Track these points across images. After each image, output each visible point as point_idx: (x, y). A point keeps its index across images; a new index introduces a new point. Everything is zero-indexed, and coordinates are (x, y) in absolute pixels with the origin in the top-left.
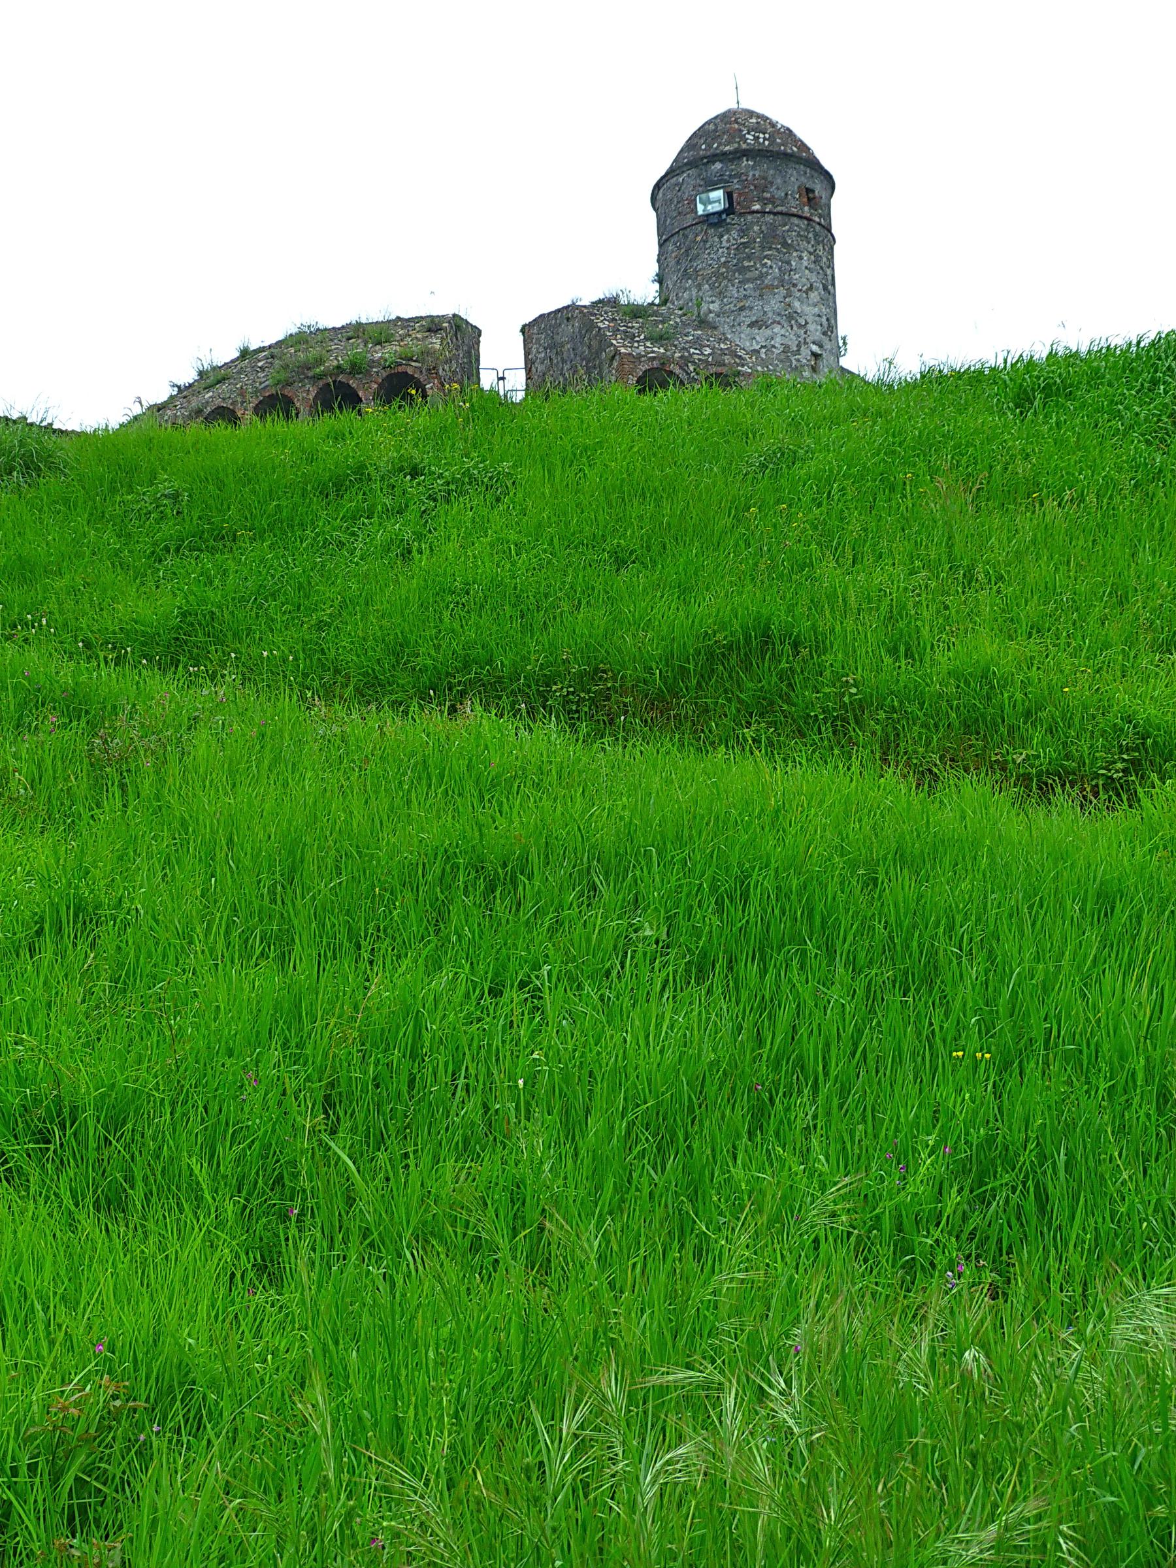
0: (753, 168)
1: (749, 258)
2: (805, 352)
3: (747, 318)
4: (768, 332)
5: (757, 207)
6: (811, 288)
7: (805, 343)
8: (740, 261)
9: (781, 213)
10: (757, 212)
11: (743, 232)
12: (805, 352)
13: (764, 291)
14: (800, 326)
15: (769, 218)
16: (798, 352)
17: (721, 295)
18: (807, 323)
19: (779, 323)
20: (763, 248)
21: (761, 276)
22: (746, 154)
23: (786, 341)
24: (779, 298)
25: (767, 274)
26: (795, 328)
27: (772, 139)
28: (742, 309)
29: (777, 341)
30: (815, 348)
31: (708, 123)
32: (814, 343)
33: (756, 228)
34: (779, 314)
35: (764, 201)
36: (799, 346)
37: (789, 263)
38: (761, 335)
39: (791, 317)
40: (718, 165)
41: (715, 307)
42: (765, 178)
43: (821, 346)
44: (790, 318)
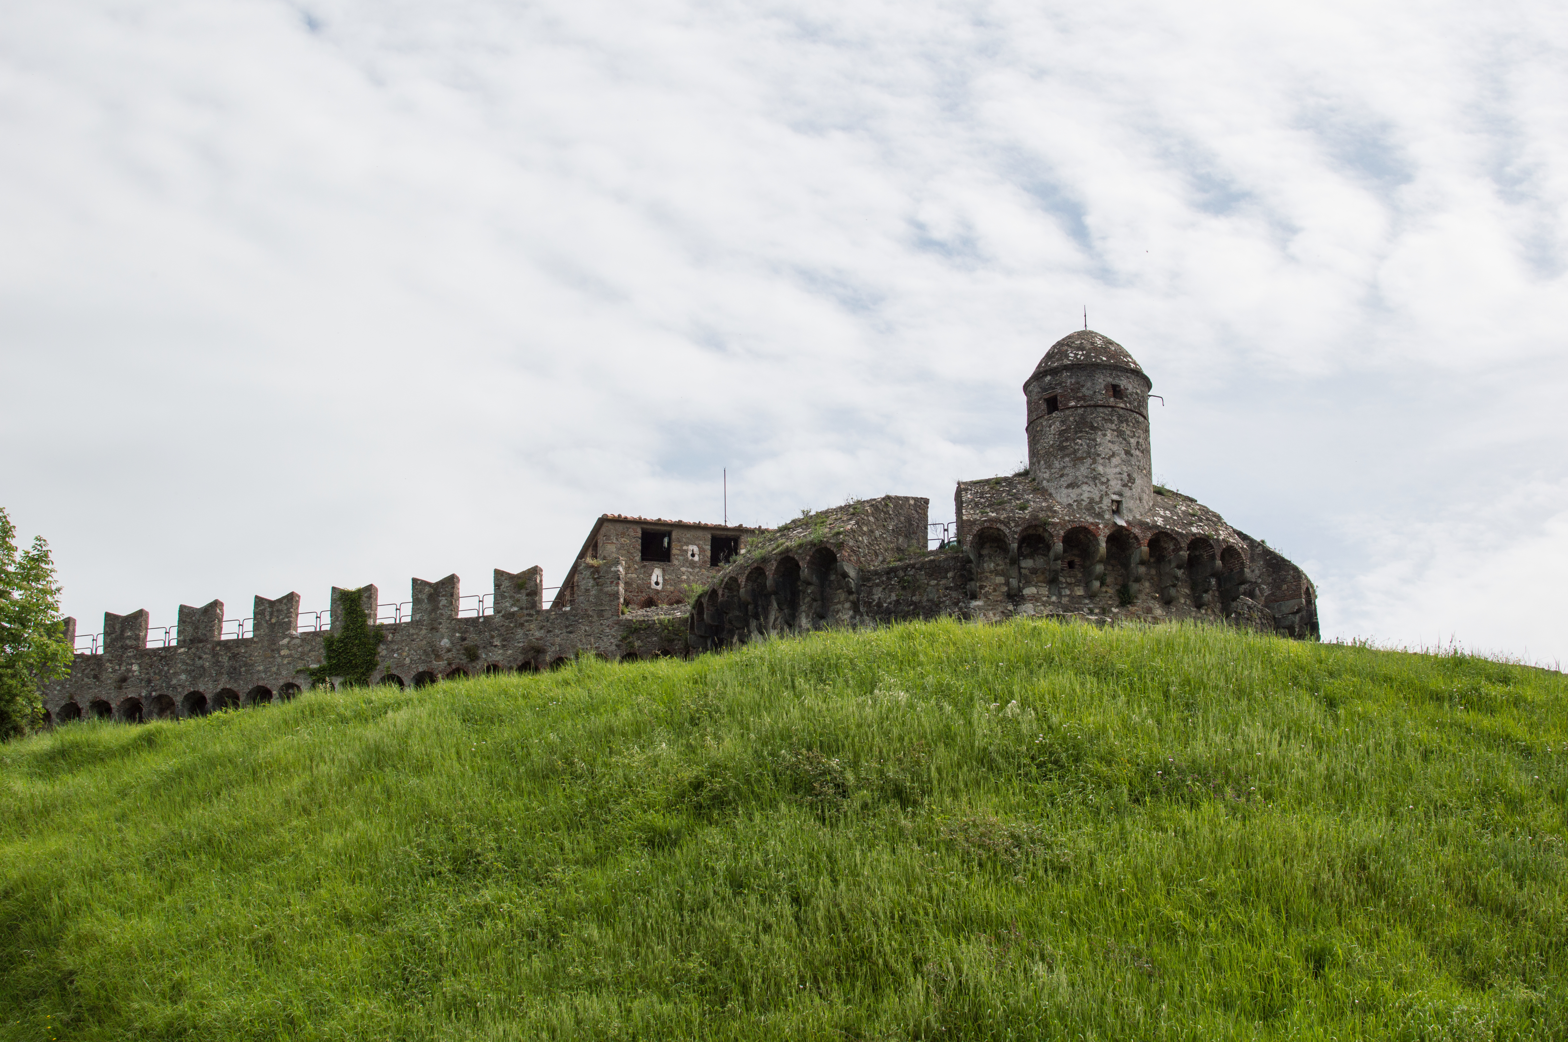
0: (1070, 377)
1: (1067, 440)
2: (1106, 502)
3: (1064, 481)
4: (1077, 491)
5: (1073, 404)
6: (1113, 455)
7: (1107, 494)
8: (1061, 442)
9: (1089, 406)
10: (1072, 407)
11: (1063, 422)
12: (1106, 502)
13: (1077, 460)
14: (1102, 483)
15: (1081, 411)
16: (1101, 501)
17: (1049, 466)
18: (1108, 480)
20: (1076, 433)
22: (1066, 368)
23: (1091, 495)
24: (1087, 465)
27: (1087, 356)
28: (1062, 476)
30: (1115, 497)
31: (1054, 347)
35: (1078, 399)
36: (1101, 498)
37: (1094, 440)
38: (1074, 493)
39: (1095, 478)
40: (1049, 378)
41: (1047, 476)
42: (1078, 383)
43: (1121, 495)
44: (1095, 478)
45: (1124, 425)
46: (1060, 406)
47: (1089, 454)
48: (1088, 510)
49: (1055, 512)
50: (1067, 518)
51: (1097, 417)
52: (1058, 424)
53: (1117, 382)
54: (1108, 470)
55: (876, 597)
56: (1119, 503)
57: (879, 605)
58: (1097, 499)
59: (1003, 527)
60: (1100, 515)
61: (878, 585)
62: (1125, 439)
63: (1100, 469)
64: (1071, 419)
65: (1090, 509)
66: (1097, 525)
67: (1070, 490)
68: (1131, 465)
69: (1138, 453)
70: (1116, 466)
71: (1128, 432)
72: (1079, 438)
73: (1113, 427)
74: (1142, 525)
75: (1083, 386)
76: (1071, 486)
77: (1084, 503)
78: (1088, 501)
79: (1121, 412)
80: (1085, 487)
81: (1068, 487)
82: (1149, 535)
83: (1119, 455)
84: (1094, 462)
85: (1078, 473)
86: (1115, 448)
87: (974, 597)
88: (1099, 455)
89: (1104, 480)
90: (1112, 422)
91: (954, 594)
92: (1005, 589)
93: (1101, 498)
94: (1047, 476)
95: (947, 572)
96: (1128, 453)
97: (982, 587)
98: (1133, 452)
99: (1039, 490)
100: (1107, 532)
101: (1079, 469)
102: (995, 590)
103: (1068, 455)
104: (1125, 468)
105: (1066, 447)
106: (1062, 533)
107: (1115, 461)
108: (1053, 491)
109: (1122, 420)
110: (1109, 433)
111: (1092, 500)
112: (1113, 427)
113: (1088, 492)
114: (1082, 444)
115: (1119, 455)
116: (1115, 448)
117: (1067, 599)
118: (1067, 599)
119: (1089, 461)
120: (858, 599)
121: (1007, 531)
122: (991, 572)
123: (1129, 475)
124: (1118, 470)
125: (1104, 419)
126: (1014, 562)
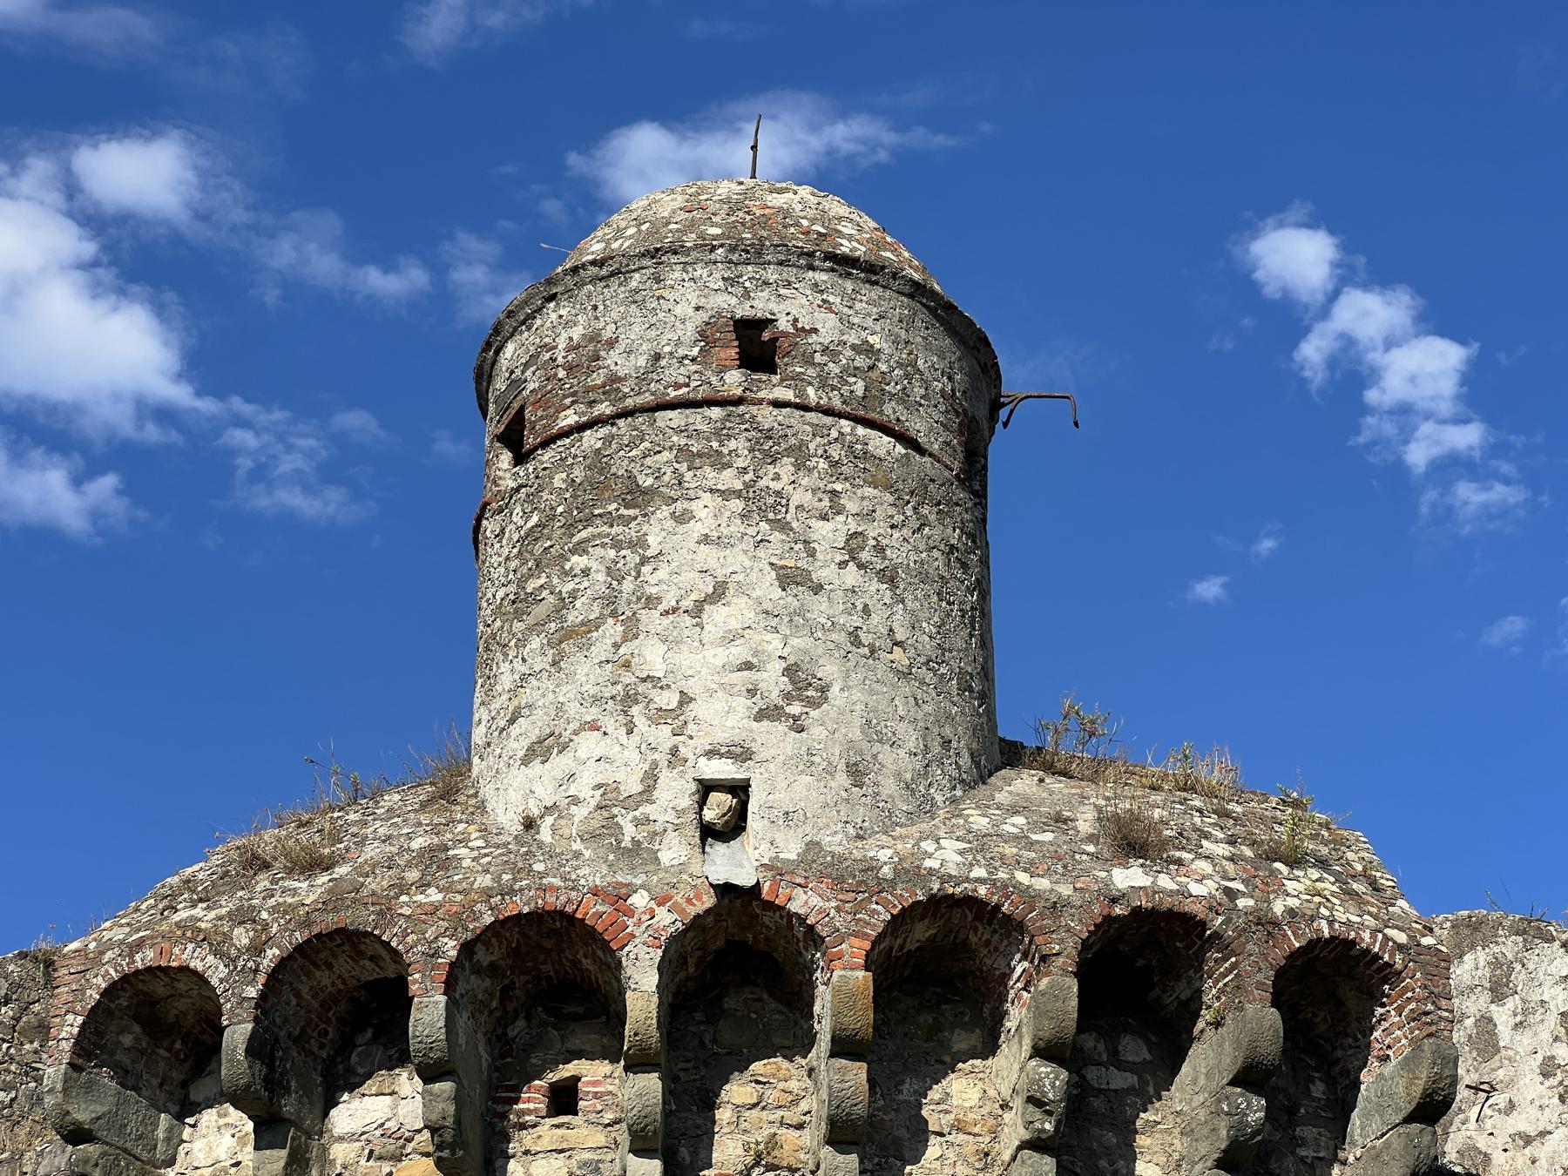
2: (675, 792)
4: (560, 764)
5: (569, 418)
6: (718, 593)
15: (591, 439)
18: (685, 699)
19: (594, 726)
20: (570, 528)
21: (565, 603)
23: (607, 775)
25: (573, 595)
26: (641, 722)
29: (583, 788)
32: (711, 753)
33: (558, 481)
34: (596, 699)
37: (639, 543)
40: (510, 348)
43: (742, 754)
45: (786, 467)
47: (610, 601)
48: (590, 837)
51: (650, 453)
53: (762, 305)
54: (686, 658)
56: (740, 790)
58: (633, 786)
60: (638, 854)
62: (783, 526)
63: (652, 656)
64: (558, 481)
65: (603, 832)
66: (619, 897)
67: (536, 767)
69: (852, 575)
70: (731, 638)
71: (798, 497)
73: (729, 479)
75: (611, 343)
76: (539, 750)
77: (579, 813)
78: (592, 799)
79: (768, 417)
80: (588, 745)
83: (741, 590)
85: (567, 693)
86: (733, 561)
88: (651, 602)
89: (669, 700)
96: (788, 578)
98: (822, 574)
100: (667, 920)
104: (774, 644)
106: (450, 948)
107: (719, 617)
109: (768, 448)
110: (704, 509)
111: (609, 798)
112: (729, 479)
113: (605, 758)
116: (733, 561)
119: (612, 629)
121: (216, 972)
123: (791, 671)
124: (739, 652)
125: (683, 452)
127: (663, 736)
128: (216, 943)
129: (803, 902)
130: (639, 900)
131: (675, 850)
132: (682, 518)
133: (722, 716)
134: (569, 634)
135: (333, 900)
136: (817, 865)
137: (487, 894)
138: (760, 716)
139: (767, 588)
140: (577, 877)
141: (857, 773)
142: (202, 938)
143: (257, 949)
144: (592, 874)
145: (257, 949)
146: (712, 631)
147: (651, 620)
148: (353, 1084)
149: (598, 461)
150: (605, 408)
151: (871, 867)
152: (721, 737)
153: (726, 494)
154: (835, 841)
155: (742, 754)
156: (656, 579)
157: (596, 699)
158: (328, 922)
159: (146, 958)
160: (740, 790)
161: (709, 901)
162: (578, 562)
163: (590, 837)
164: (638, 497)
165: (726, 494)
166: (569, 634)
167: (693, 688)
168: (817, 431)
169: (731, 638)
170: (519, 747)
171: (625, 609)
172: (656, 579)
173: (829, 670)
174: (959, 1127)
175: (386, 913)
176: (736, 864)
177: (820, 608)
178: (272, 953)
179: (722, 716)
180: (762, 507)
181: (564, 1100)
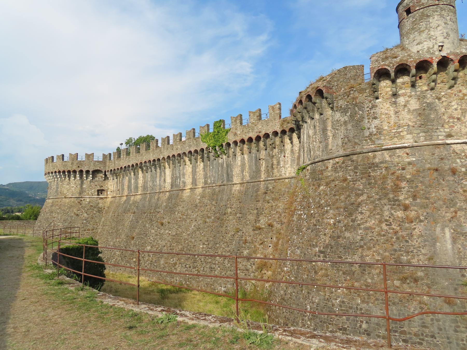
2: (436, 47)
3: (415, 43)
4: (421, 45)
5: (418, 8)
6: (439, 26)
7: (436, 43)
13: (421, 32)
14: (434, 39)
16: (433, 47)
18: (436, 37)
20: (420, 20)
21: (420, 29)
23: (428, 46)
29: (425, 47)
34: (426, 38)
35: (420, 6)
36: (433, 46)
37: (429, 21)
38: (420, 47)
43: (443, 42)
46: (412, 11)
47: (426, 28)
48: (427, 52)
49: (411, 56)
50: (417, 58)
52: (411, 19)
55: (340, 104)
57: (341, 107)
58: (432, 47)
59: (387, 67)
60: (433, 53)
61: (340, 100)
62: (444, 18)
63: (432, 33)
65: (428, 51)
66: (432, 58)
67: (418, 46)
68: (448, 28)
69: (451, 23)
70: (440, 30)
71: (445, 14)
72: (422, 22)
73: (438, 13)
74: (456, 54)
76: (418, 44)
77: (425, 50)
79: (441, 6)
80: (425, 43)
81: (417, 45)
82: (459, 58)
83: (441, 25)
84: (429, 31)
86: (440, 22)
87: (377, 98)
88: (431, 27)
89: (435, 37)
90: (437, 12)
91: (369, 98)
92: (391, 93)
93: (433, 46)
94: (407, 43)
95: (366, 90)
96: (445, 23)
97: (381, 94)
98: (448, 23)
99: (403, 49)
100: (437, 60)
101: (422, 36)
102: (386, 94)
103: (416, 31)
104: (445, 31)
105: (415, 28)
106: (415, 64)
107: (439, 28)
108: (410, 48)
109: (442, 9)
110: (436, 17)
111: (429, 48)
112: (438, 13)
113: (426, 45)
114: (423, 25)
115: (441, 25)
116: (440, 22)
117: (419, 92)
118: (419, 92)
119: (427, 31)
120: (333, 106)
121: (389, 68)
122: (384, 87)
123: (447, 33)
124: (441, 32)
126: (393, 81)
127: (434, 41)
128: (389, 66)
129: (451, 57)
130: (434, 58)
131: (437, 53)
132: (434, 18)
133: (440, 39)
134: (421, 31)
135: (401, 60)
136: (451, 53)
137: (418, 59)
138: (444, 38)
139: (443, 24)
140: (427, 57)
141: (453, 43)
142: (386, 65)
143: (393, 66)
144: (428, 56)
145: (393, 66)
146: (438, 30)
147: (432, 29)
148: (398, 78)
149: (422, 13)
150: (422, 7)
151: (458, 53)
152: (441, 41)
153: (438, 15)
154: (452, 50)
155: (443, 42)
156: (431, 25)
157: (426, 38)
158: (401, 63)
159: (380, 68)
160: (442, 46)
161: (441, 58)
162: (422, 24)
163: (427, 52)
164: (428, 16)
165: (438, 15)
166: (421, 31)
167: (437, 36)
168: (446, 7)
169: (440, 30)
170: (416, 44)
171: (428, 28)
172: (431, 25)
173: (450, 33)
174: (461, 77)
175: (407, 61)
176: (444, 54)
177: (449, 26)
178: (395, 66)
179: (440, 39)
180: (442, 16)
181: (420, 78)
